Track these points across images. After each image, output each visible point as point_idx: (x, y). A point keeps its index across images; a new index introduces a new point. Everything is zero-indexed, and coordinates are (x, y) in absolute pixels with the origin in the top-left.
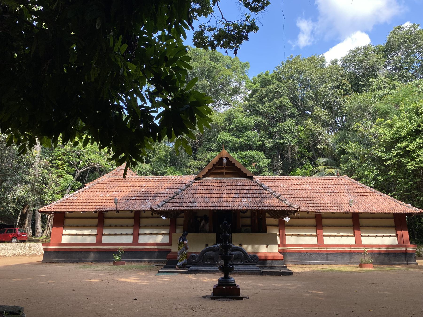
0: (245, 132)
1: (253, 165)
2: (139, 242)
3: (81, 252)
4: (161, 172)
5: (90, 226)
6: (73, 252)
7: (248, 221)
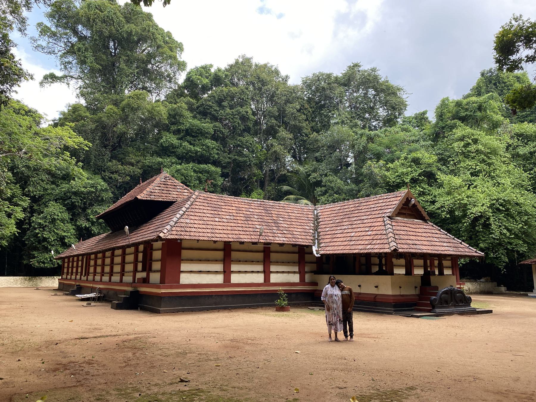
0: (200, 140)
1: (209, 182)
2: (271, 282)
3: (212, 296)
5: (216, 261)
6: (201, 296)
7: (363, 260)
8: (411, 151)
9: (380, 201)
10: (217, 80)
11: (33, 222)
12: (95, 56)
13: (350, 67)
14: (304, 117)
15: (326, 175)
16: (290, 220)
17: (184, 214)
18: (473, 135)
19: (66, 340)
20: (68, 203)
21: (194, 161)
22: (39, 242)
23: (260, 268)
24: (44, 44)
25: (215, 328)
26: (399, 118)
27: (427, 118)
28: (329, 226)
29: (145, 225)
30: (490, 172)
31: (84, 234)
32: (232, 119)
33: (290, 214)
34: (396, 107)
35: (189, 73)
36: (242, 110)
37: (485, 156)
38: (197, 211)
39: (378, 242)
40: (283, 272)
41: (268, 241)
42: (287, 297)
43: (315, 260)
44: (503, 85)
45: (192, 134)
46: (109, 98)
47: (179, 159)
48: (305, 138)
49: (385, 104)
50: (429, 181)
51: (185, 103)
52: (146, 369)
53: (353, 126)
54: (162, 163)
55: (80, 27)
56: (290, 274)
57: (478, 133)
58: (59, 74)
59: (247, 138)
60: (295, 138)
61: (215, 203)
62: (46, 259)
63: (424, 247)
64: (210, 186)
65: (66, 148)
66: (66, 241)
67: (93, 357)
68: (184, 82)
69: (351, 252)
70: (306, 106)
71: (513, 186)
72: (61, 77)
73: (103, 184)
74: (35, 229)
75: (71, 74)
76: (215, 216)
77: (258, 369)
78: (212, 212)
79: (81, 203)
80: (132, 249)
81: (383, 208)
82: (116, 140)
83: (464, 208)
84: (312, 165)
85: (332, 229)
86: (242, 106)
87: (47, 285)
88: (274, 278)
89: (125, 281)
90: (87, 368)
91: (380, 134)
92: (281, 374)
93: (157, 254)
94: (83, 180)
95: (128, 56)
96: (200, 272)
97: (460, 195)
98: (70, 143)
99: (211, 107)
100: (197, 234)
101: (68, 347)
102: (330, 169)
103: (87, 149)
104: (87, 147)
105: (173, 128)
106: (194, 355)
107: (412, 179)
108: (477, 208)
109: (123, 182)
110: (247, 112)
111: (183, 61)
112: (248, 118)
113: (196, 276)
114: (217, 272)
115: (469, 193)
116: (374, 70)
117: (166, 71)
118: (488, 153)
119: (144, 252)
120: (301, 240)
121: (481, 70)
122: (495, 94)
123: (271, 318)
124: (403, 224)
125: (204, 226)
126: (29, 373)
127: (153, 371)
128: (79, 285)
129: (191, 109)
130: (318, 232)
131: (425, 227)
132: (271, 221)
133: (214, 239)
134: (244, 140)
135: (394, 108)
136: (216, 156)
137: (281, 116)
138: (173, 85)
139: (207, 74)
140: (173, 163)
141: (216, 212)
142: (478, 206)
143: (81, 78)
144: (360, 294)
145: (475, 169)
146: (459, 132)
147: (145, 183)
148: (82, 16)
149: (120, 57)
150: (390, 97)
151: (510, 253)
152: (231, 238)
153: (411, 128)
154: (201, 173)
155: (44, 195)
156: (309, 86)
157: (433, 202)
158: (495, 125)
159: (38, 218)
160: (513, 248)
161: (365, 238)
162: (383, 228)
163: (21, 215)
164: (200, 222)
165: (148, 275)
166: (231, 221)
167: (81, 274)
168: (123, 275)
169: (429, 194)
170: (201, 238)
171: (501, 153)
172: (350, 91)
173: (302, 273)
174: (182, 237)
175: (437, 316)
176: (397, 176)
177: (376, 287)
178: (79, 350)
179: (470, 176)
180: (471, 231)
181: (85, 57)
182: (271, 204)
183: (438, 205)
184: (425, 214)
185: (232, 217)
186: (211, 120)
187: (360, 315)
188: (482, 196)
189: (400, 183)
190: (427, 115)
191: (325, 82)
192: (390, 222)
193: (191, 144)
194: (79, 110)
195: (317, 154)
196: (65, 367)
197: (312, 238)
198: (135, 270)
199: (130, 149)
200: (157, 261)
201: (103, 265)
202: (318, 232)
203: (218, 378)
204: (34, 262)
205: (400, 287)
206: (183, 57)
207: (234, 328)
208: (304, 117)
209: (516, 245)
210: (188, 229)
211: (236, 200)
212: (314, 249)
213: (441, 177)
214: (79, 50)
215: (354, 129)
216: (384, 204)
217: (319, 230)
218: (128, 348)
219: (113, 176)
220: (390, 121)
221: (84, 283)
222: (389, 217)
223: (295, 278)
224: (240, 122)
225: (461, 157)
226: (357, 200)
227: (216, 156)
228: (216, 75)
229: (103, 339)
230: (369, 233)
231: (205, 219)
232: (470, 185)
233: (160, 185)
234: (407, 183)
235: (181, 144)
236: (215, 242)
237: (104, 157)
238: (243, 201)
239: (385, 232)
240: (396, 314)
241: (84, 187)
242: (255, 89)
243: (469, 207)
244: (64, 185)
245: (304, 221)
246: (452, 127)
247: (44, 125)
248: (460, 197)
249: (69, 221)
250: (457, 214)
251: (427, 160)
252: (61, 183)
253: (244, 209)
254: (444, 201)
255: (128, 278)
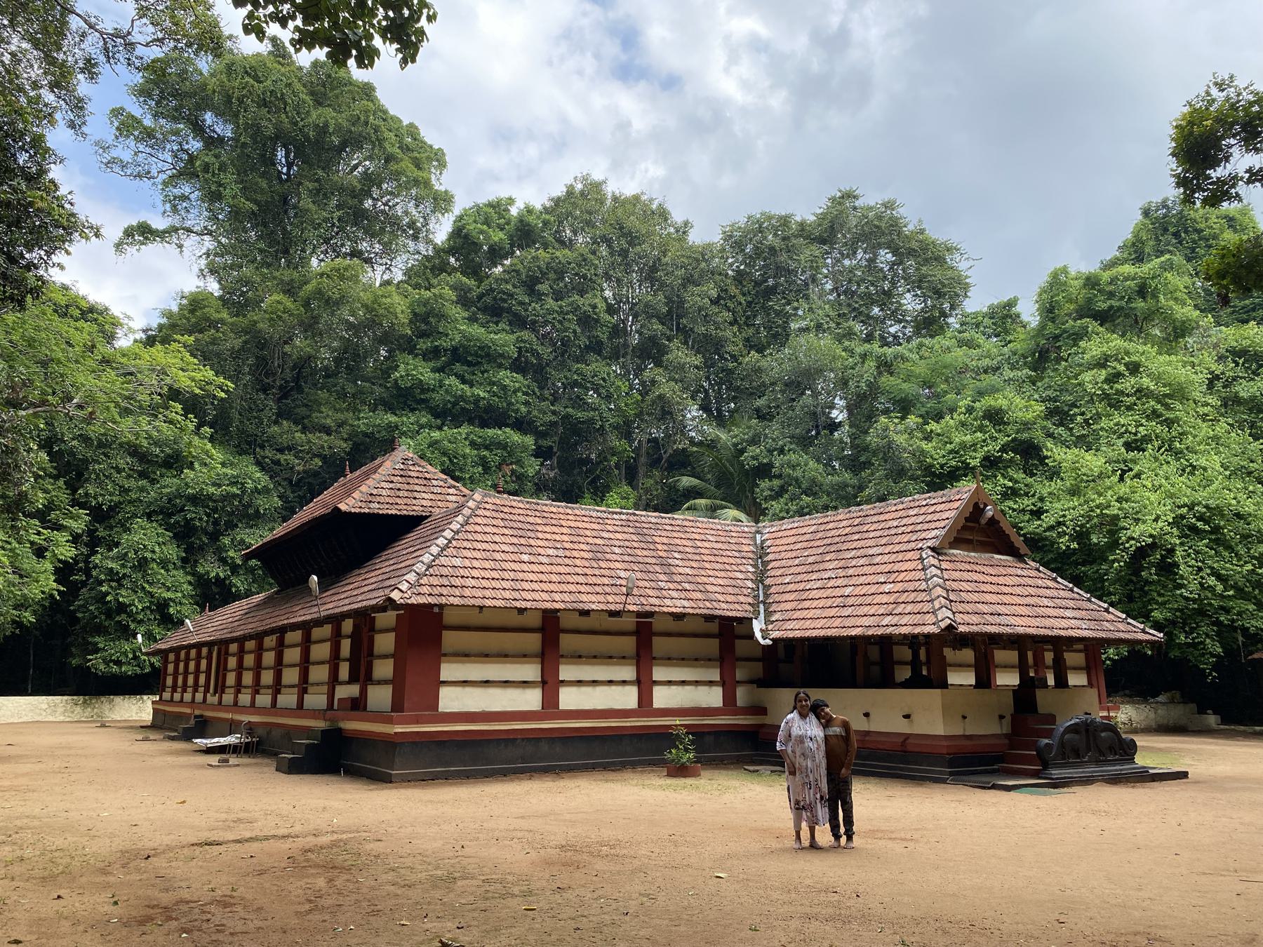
0: (486, 371)
1: (507, 470)
2: (655, 706)
4: (167, 449)
5: (525, 656)
6: (489, 741)
7: (874, 653)
8: (981, 394)
9: (912, 512)
10: (525, 233)
11: (96, 567)
12: (242, 182)
13: (833, 199)
14: (728, 316)
15: (781, 451)
16: (697, 557)
17: (447, 546)
18: (1127, 353)
19: (169, 848)
20: (178, 522)
21: (471, 421)
22: (109, 614)
23: (628, 673)
24: (126, 156)
25: (523, 817)
26: (951, 315)
27: (1018, 316)
28: (792, 570)
29: (357, 572)
30: (1171, 441)
31: (212, 595)
32: (560, 322)
33: (699, 544)
34: (943, 291)
35: (460, 218)
36: (584, 302)
37: (1159, 402)
38: (479, 537)
39: (909, 608)
40: (683, 683)
41: (648, 608)
42: (692, 742)
43: (759, 653)
44: (1196, 237)
45: (467, 358)
46: (275, 278)
47: (436, 416)
48: (731, 365)
49: (918, 283)
50: (1027, 463)
51: (453, 288)
52: (359, 917)
53: (844, 336)
54: (397, 427)
55: (209, 117)
56: (700, 688)
57: (1139, 349)
58: (159, 223)
59: (596, 367)
60: (708, 364)
61: (521, 518)
62: (125, 654)
63: (1019, 621)
64: (508, 479)
65: (174, 394)
66: (171, 610)
67: (233, 890)
68: (449, 240)
69: (845, 633)
70: (733, 290)
71: (1227, 473)
72: (164, 232)
73: (258, 477)
74: (100, 583)
75: (188, 224)
76: (522, 549)
77: (627, 918)
78: (515, 540)
79: (207, 522)
80: (327, 630)
81: (919, 527)
82: (288, 375)
83: (1112, 525)
84: (749, 427)
85: (799, 578)
86: (582, 293)
87: (126, 717)
88: (663, 697)
89: (311, 707)
90: (218, 915)
91: (907, 354)
92: (682, 929)
93: (385, 642)
94: (213, 467)
95: (318, 180)
96: (487, 683)
97: (1100, 494)
98: (183, 381)
99: (511, 295)
100: (479, 593)
101: (173, 864)
102: (792, 437)
103: (223, 395)
104: (223, 390)
105: (424, 344)
106: (475, 882)
107: (986, 458)
108: (1142, 527)
109: (304, 471)
110: (594, 307)
111: (446, 192)
112: (597, 321)
113: (476, 693)
114: (525, 684)
115: (1123, 490)
116: (889, 205)
117: (406, 213)
118: (1165, 396)
119: (355, 637)
120: (724, 606)
121: (1142, 203)
122: (1178, 259)
123: (656, 793)
124: (968, 567)
125: (495, 574)
126: (81, 928)
127: (376, 922)
128: (201, 716)
129: (464, 300)
130: (765, 586)
131: (1019, 572)
132: (654, 561)
133: (518, 604)
134: (588, 370)
135: (939, 294)
136: (523, 409)
137: (674, 315)
138: (422, 247)
139: (502, 221)
140: (422, 427)
141: (523, 541)
142: (1144, 522)
143: (210, 233)
144: (868, 733)
145: (1135, 434)
146: (1093, 348)
147: (358, 473)
148: (214, 91)
149: (300, 183)
150: (929, 267)
151: (1225, 632)
152: (558, 601)
153: (981, 340)
154: (487, 448)
155: (120, 503)
156: (738, 246)
157: (1037, 514)
158: (1179, 331)
159: (107, 558)
160: (1233, 621)
161: (878, 599)
162: (920, 575)
163: (67, 552)
164: (487, 565)
165: (364, 692)
166: (559, 561)
167: (207, 691)
168: (305, 691)
169: (1026, 494)
170: (488, 603)
171: (1197, 395)
172: (836, 254)
173: (728, 685)
174: (443, 600)
175: (1055, 786)
176: (951, 452)
177: (907, 717)
178: (202, 871)
179: (1123, 450)
180: (1131, 581)
181: (220, 185)
182: (653, 520)
183: (1048, 520)
184: (1018, 542)
185: (561, 553)
186: (510, 324)
187: (868, 786)
188: (1153, 497)
189: (958, 468)
190: (1018, 309)
191: (776, 235)
192: (935, 562)
193: (464, 382)
194: (205, 306)
195: (760, 402)
196: (168, 913)
197: (750, 600)
198: (334, 680)
199: (323, 395)
200: (386, 657)
201: (258, 668)
202: (765, 586)
203: (531, 938)
204: (96, 663)
205: (964, 717)
206: (442, 182)
207: (568, 817)
208: (728, 316)
209: (1239, 614)
210: (458, 582)
211: (569, 511)
212: (757, 626)
213: (1056, 453)
214: (206, 168)
215: (847, 343)
216: (921, 519)
217: (768, 582)
218: (317, 866)
219: (282, 458)
220: (929, 324)
221: (214, 710)
222: (933, 549)
223: (713, 697)
224: (579, 330)
225: (1100, 407)
226: (858, 508)
227: (523, 409)
228: (521, 221)
229: (256, 845)
230: (887, 588)
231: (497, 556)
232: (1124, 472)
233: (392, 478)
234: (974, 468)
235: (441, 381)
236: (521, 611)
237: (262, 415)
238: (587, 513)
239: (924, 586)
240: (956, 782)
241: (214, 484)
242: (612, 254)
243: (1123, 524)
244: (168, 481)
245: (731, 560)
246: (1077, 336)
247: (123, 342)
248: (1102, 500)
249: (179, 564)
250: (1095, 540)
251: (1021, 414)
252: (162, 476)
253: (588, 533)
254: (1063, 510)
255: (317, 699)
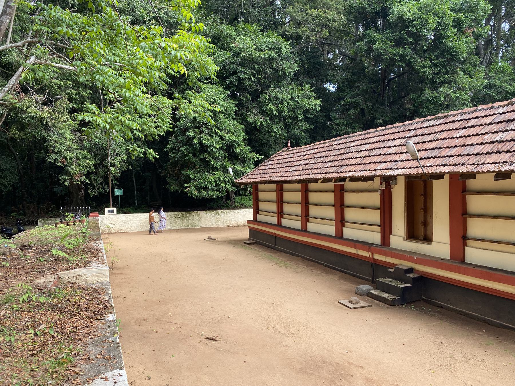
20: (232, 83)
74: (187, 129)
204: (191, 189)
241: (259, 50)
